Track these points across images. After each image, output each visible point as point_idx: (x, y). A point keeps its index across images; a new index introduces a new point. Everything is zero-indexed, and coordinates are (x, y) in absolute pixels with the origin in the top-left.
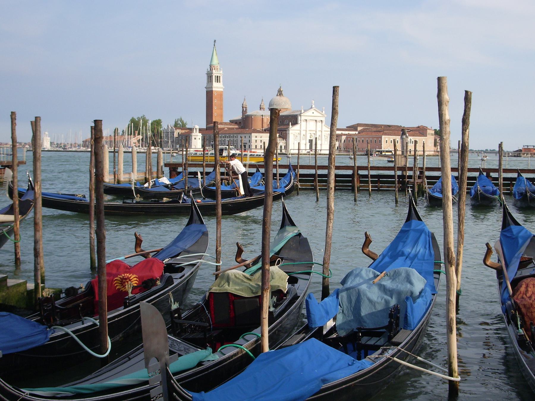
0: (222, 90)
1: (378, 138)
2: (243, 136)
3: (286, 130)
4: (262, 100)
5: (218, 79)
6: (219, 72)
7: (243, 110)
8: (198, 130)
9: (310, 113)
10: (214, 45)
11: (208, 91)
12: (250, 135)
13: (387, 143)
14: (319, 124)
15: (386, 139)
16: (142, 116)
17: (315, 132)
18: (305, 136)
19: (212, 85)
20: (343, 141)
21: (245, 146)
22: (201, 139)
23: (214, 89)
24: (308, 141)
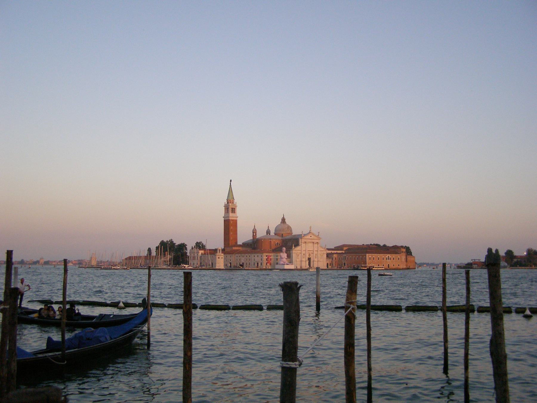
1: (363, 256)
2: (256, 255)
3: (290, 251)
4: (268, 226)
5: (233, 210)
6: (234, 205)
7: (253, 234)
8: (221, 251)
9: (309, 237)
10: (230, 184)
11: (225, 220)
12: (261, 255)
13: (370, 259)
15: (370, 257)
19: (229, 215)
21: (258, 263)
22: (223, 258)
23: (230, 219)
24: (307, 259)
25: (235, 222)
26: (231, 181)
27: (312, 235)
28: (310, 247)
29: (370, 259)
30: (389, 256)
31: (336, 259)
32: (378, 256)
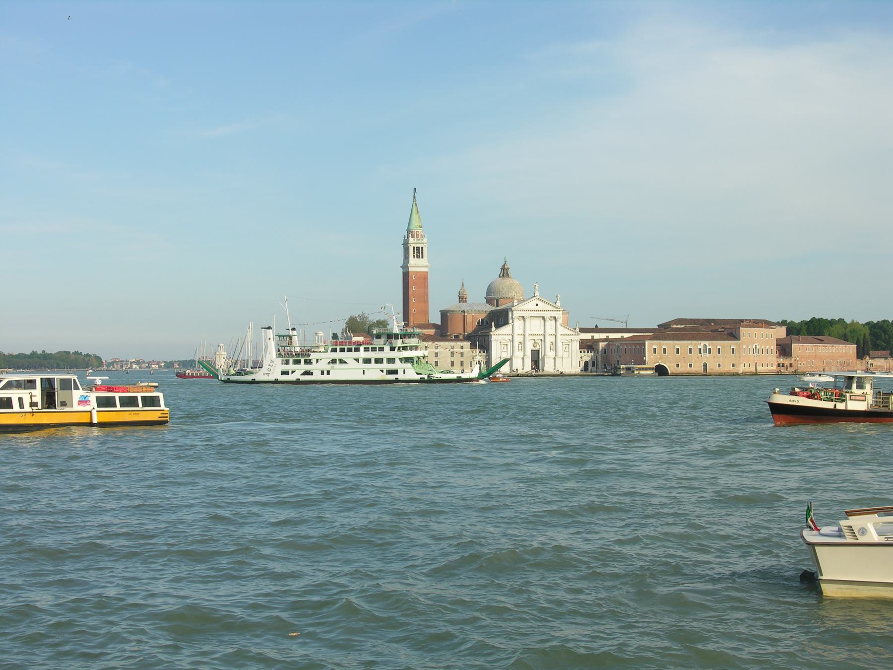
0: (426, 270)
1: (640, 344)
3: (488, 336)
5: (419, 252)
9: (531, 305)
10: (414, 197)
13: (655, 352)
14: (550, 324)
15: (654, 347)
16: (361, 314)
17: (543, 338)
18: (523, 344)
19: (408, 262)
20: (600, 353)
23: (410, 269)
24: (529, 354)
25: (423, 278)
26: (415, 189)
27: (539, 302)
28: (535, 327)
29: (655, 352)
30: (707, 345)
31: (605, 353)
32: (677, 344)
